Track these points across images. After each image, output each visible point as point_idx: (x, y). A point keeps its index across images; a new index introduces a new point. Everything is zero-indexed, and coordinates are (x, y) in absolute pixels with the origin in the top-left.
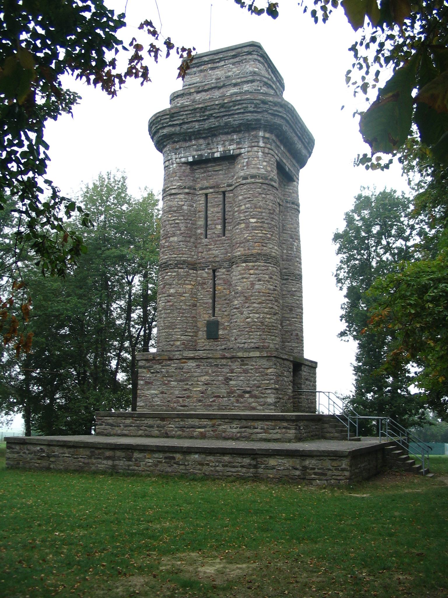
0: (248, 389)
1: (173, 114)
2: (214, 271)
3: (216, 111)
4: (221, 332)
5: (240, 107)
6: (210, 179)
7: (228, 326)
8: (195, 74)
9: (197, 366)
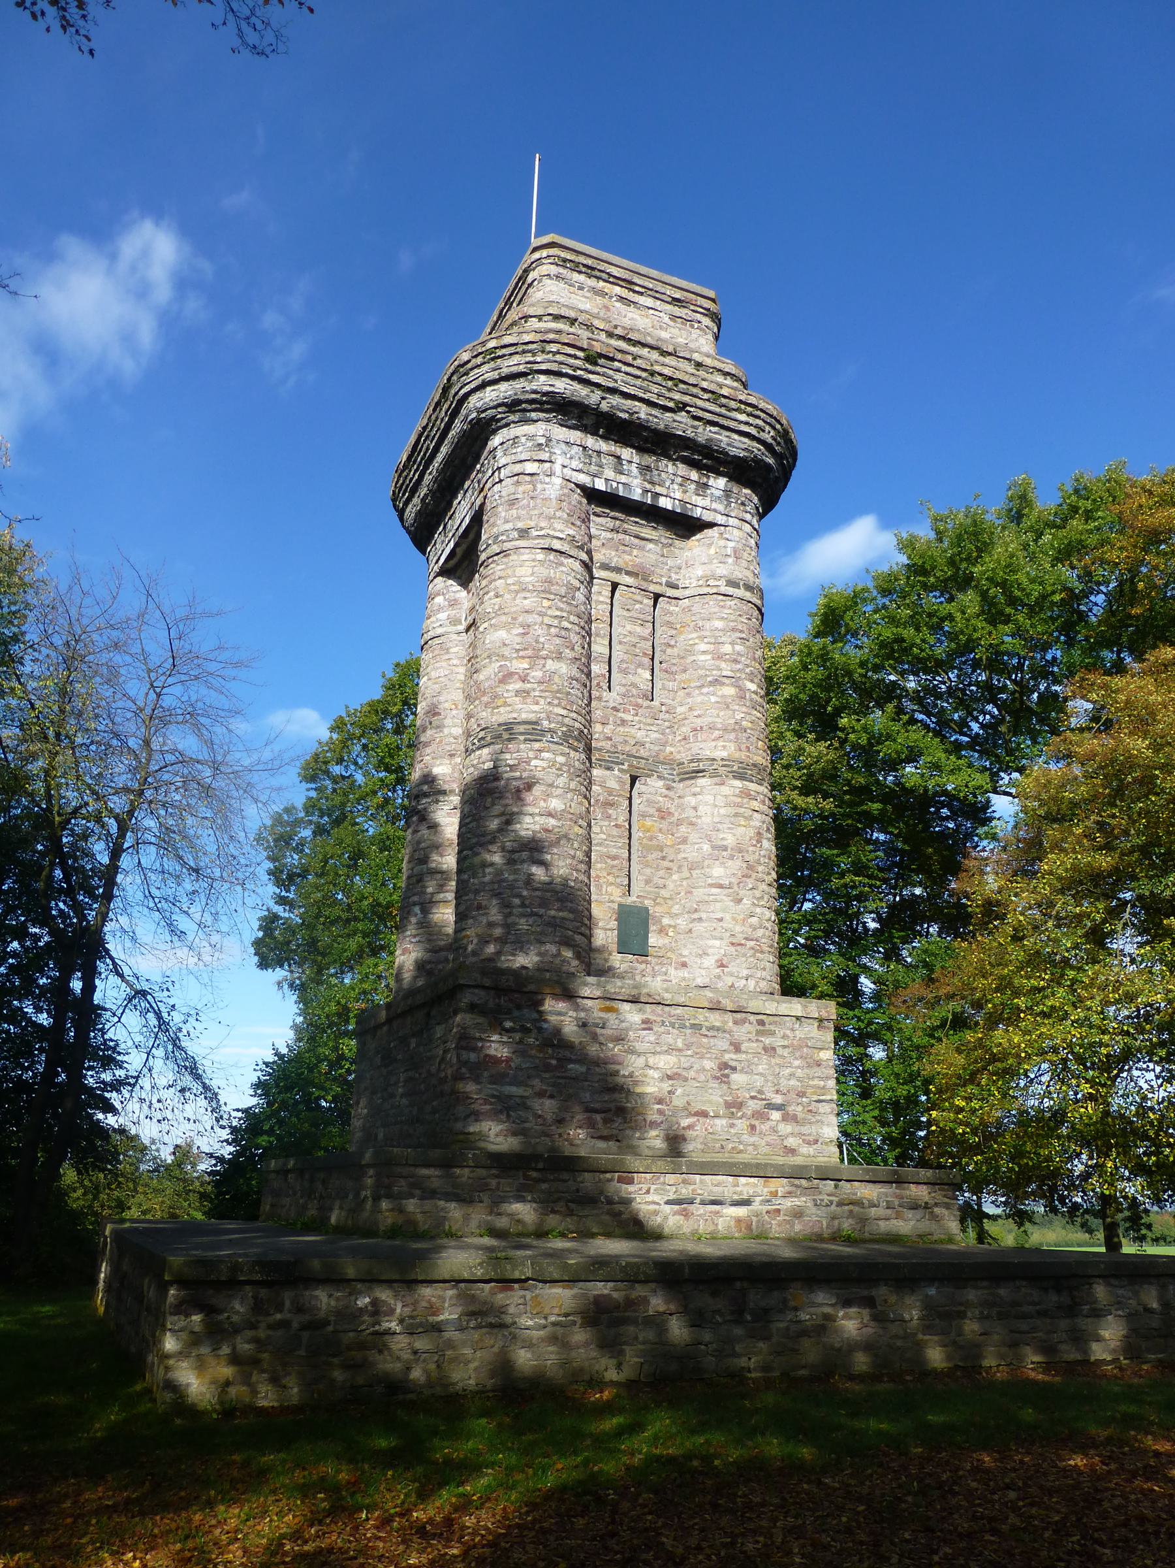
0: (778, 1099)
1: (601, 356)
2: (634, 780)
3: (700, 403)
4: (652, 940)
5: (751, 420)
6: (624, 552)
7: (670, 926)
8: (581, 288)
9: (644, 1022)
